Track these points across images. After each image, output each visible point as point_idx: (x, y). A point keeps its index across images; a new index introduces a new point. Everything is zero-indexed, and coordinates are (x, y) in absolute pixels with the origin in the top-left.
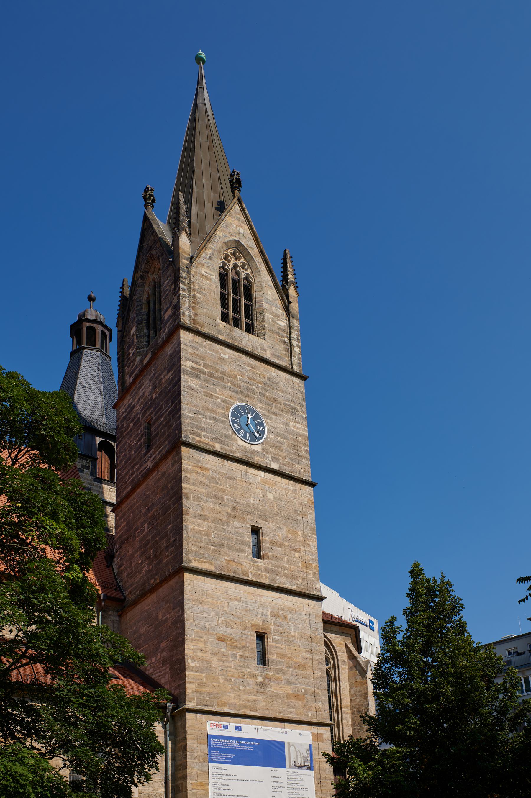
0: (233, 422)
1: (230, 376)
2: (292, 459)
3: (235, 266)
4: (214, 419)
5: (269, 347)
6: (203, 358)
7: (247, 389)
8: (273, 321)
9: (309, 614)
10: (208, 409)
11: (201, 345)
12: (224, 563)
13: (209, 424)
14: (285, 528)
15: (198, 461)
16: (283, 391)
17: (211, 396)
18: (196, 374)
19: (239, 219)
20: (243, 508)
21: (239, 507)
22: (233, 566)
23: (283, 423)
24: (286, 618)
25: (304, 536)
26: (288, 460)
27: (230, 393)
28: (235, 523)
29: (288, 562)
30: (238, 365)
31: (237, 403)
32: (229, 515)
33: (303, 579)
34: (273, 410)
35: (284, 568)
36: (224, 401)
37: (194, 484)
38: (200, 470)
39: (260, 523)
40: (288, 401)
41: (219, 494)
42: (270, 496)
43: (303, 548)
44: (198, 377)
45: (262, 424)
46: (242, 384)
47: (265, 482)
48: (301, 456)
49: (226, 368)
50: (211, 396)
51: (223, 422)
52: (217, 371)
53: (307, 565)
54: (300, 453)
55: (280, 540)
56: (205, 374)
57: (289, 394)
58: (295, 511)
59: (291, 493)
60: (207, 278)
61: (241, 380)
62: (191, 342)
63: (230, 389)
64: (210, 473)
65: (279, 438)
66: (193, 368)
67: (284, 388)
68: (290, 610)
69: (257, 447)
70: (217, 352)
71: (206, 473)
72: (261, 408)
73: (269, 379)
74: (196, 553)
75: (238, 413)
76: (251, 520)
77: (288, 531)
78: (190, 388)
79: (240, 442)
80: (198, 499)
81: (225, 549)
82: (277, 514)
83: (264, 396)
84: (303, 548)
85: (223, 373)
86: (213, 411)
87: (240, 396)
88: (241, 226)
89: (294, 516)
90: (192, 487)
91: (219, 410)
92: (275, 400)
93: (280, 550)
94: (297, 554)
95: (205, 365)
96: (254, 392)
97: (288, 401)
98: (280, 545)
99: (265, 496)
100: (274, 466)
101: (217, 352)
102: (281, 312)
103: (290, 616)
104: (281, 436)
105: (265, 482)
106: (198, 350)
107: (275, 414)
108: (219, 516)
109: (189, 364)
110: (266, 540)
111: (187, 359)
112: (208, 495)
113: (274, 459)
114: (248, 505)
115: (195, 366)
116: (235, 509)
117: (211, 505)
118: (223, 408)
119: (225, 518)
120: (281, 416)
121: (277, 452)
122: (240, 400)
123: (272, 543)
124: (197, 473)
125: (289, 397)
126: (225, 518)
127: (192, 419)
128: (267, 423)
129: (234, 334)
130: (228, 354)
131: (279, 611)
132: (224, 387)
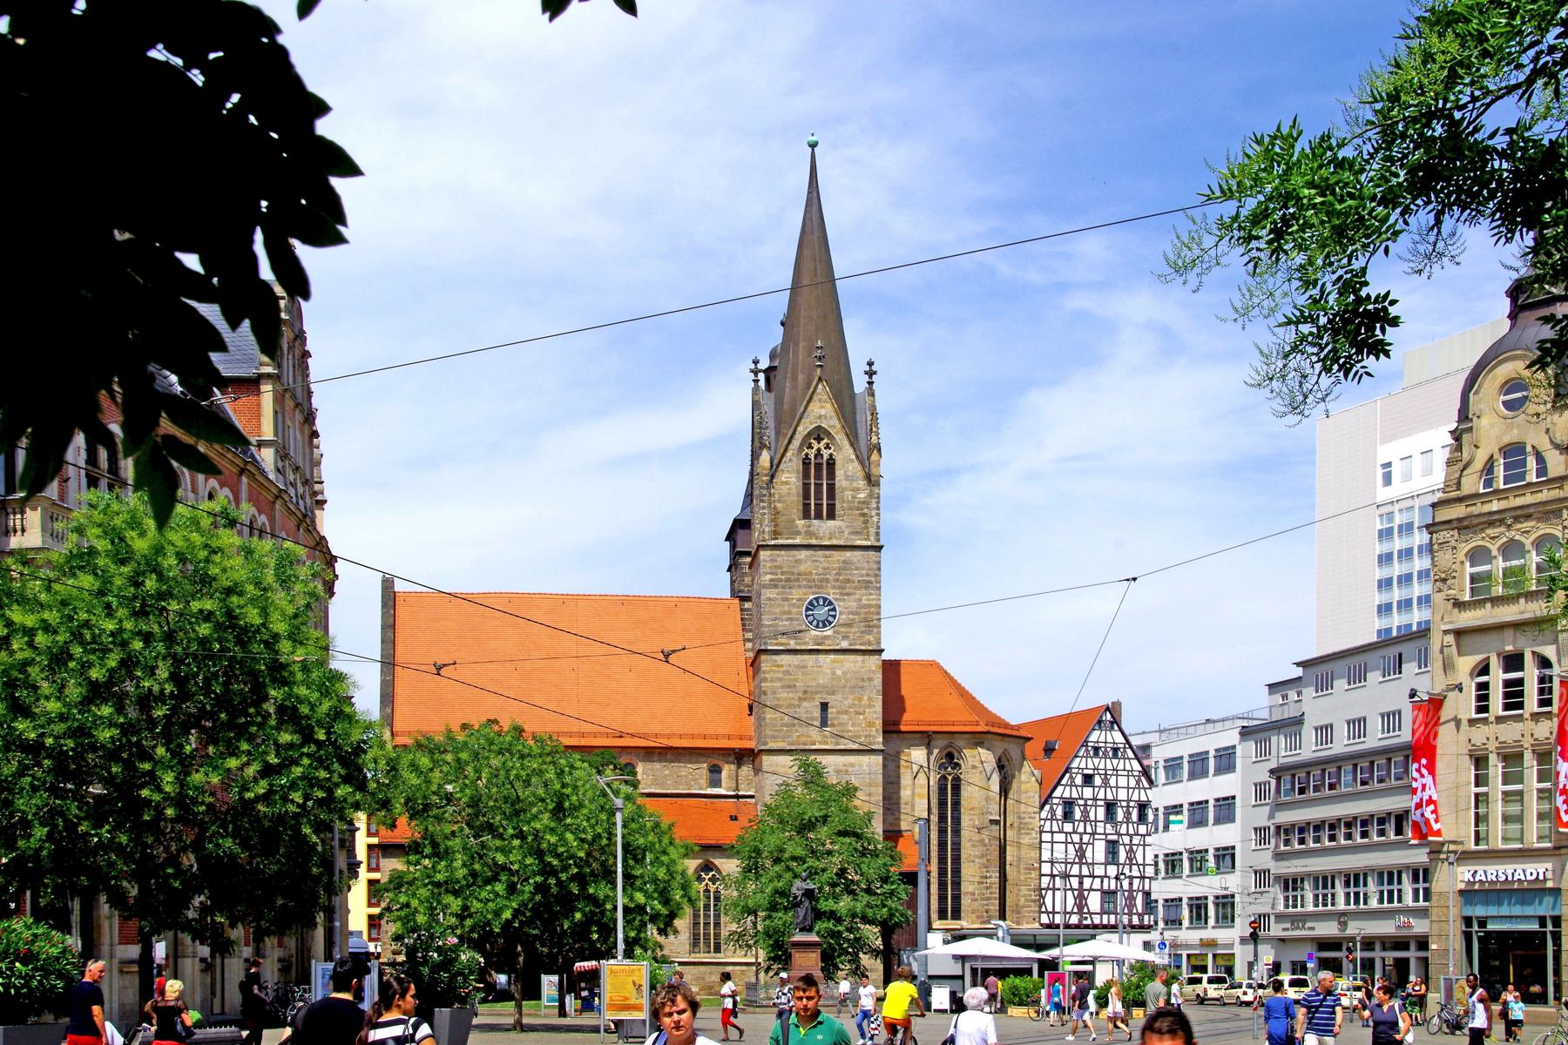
0: (807, 616)
1: (805, 574)
2: (862, 632)
3: (819, 450)
4: (790, 619)
5: (847, 527)
6: (780, 567)
7: (821, 580)
8: (853, 497)
9: (869, 765)
10: (785, 613)
11: (779, 556)
12: (795, 738)
13: (785, 625)
14: (852, 697)
15: (775, 661)
16: (857, 569)
17: (786, 599)
18: (774, 584)
19: (820, 400)
20: (813, 689)
21: (809, 689)
22: (803, 739)
23: (855, 601)
24: (847, 771)
25: (870, 699)
26: (858, 634)
27: (804, 590)
28: (805, 704)
29: (853, 725)
30: (814, 561)
31: (812, 597)
32: (800, 699)
33: (866, 736)
34: (846, 591)
35: (850, 731)
36: (799, 600)
37: (771, 681)
38: (776, 669)
39: (828, 698)
40: (862, 576)
41: (792, 683)
42: (839, 673)
43: (867, 710)
44: (776, 586)
45: (834, 609)
46: (817, 577)
47: (834, 661)
48: (872, 626)
49: (802, 568)
50: (786, 599)
51: (797, 619)
52: (793, 574)
53: (870, 724)
54: (871, 624)
55: (845, 708)
56: (781, 580)
57: (864, 569)
58: (863, 680)
59: (859, 664)
60: (787, 483)
61: (816, 574)
62: (771, 555)
63: (805, 587)
64: (785, 668)
65: (851, 617)
66: (771, 580)
67: (859, 565)
68: (852, 765)
69: (828, 632)
70: (794, 556)
71: (781, 669)
72: (834, 594)
73: (844, 562)
74: (773, 737)
75: (811, 606)
76: (818, 699)
77: (854, 699)
78: (769, 599)
79: (813, 633)
80: (775, 693)
81: (796, 728)
82: (844, 687)
83: (837, 580)
84: (867, 710)
85: (799, 574)
86: (789, 612)
87: (814, 590)
88: (822, 407)
89: (861, 684)
90: (769, 684)
91: (794, 610)
92: (849, 581)
93: (846, 717)
94: (861, 717)
95: (782, 574)
96: (828, 581)
97: (862, 576)
98: (846, 712)
99: (834, 673)
100: (845, 645)
101: (794, 556)
102: (862, 483)
103: (850, 769)
104: (852, 613)
105: (834, 661)
106: (776, 561)
107: (848, 594)
108: (793, 702)
109: (769, 577)
110: (832, 713)
111: (767, 573)
112: (783, 687)
113: (845, 637)
114: (818, 686)
115: (773, 577)
116: (805, 692)
117: (785, 695)
118: (798, 607)
119: (797, 702)
120: (854, 594)
121: (848, 629)
122: (814, 593)
123: (838, 712)
124: (774, 672)
125: (864, 572)
126: (797, 702)
127: (770, 626)
128: (839, 606)
129: (811, 529)
130: (803, 554)
131: (842, 768)
132: (800, 587)
